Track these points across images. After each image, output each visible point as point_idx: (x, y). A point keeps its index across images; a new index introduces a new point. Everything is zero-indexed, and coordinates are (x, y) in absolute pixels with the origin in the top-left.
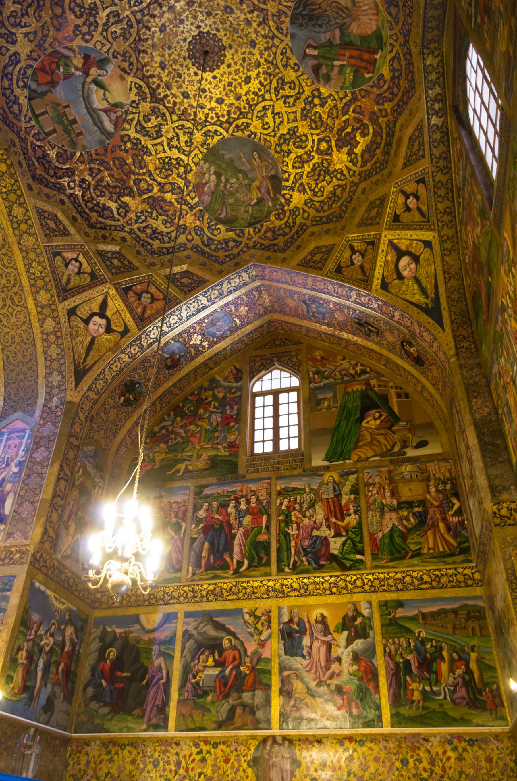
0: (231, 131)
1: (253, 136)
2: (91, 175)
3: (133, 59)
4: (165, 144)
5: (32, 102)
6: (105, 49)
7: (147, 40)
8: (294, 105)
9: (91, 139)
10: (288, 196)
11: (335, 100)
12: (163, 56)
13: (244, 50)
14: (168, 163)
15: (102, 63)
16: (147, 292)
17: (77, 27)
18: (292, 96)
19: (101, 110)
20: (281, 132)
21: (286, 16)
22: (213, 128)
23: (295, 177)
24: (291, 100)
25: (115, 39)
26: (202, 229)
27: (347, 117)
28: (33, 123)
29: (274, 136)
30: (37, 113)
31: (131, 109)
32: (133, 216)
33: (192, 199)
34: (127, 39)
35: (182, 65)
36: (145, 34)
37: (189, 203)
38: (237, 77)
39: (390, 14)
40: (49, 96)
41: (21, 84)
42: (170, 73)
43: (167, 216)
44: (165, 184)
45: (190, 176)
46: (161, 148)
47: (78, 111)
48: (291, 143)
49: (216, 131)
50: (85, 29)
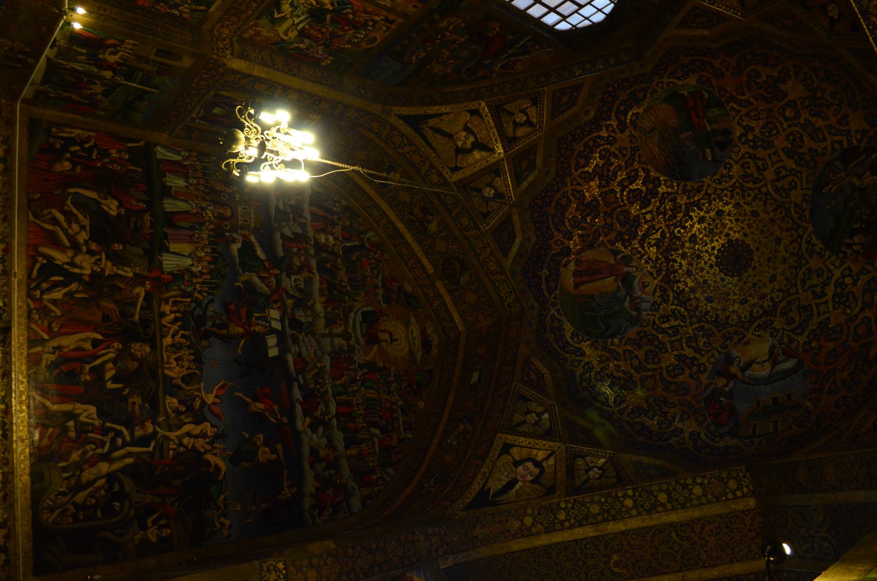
0: (805, 225)
1: (807, 198)
3: (732, 330)
4: (819, 301)
6: (717, 355)
7: (717, 315)
8: (763, 159)
10: (858, 136)
11: (741, 118)
12: (734, 301)
13: (728, 221)
15: (729, 360)
17: (691, 376)
18: (756, 164)
20: (794, 166)
21: (685, 186)
22: (804, 245)
23: (835, 134)
24: (760, 163)
25: (710, 345)
27: (751, 99)
29: (801, 173)
31: (778, 338)
34: (713, 333)
35: (746, 283)
36: (711, 317)
38: (754, 225)
39: (645, 97)
41: (717, 439)
42: (750, 296)
45: (855, 269)
48: (801, 151)
49: (808, 242)
50: (695, 369)
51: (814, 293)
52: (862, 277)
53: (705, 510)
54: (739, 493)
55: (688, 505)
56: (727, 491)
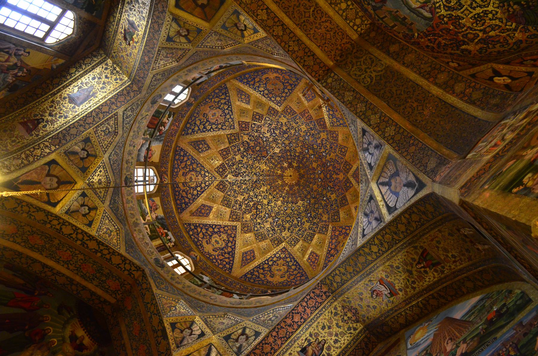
2: (431, 43)
4: (469, 8)
5: (376, 12)
9: (420, 25)
14: (478, 17)
16: (527, 61)
19: (418, 8)
26: (534, 35)
28: (381, 21)
30: (381, 17)
32: (476, 52)
33: (511, 26)
37: (511, 29)
40: (384, 8)
41: (366, 2)
43: (501, 43)
44: (485, 29)
45: (499, 15)
46: (468, 12)
47: (404, 12)
51: (472, 4)
52: (497, 21)
53: (336, 17)
54: (355, 28)
55: (333, 6)
56: (353, 21)
